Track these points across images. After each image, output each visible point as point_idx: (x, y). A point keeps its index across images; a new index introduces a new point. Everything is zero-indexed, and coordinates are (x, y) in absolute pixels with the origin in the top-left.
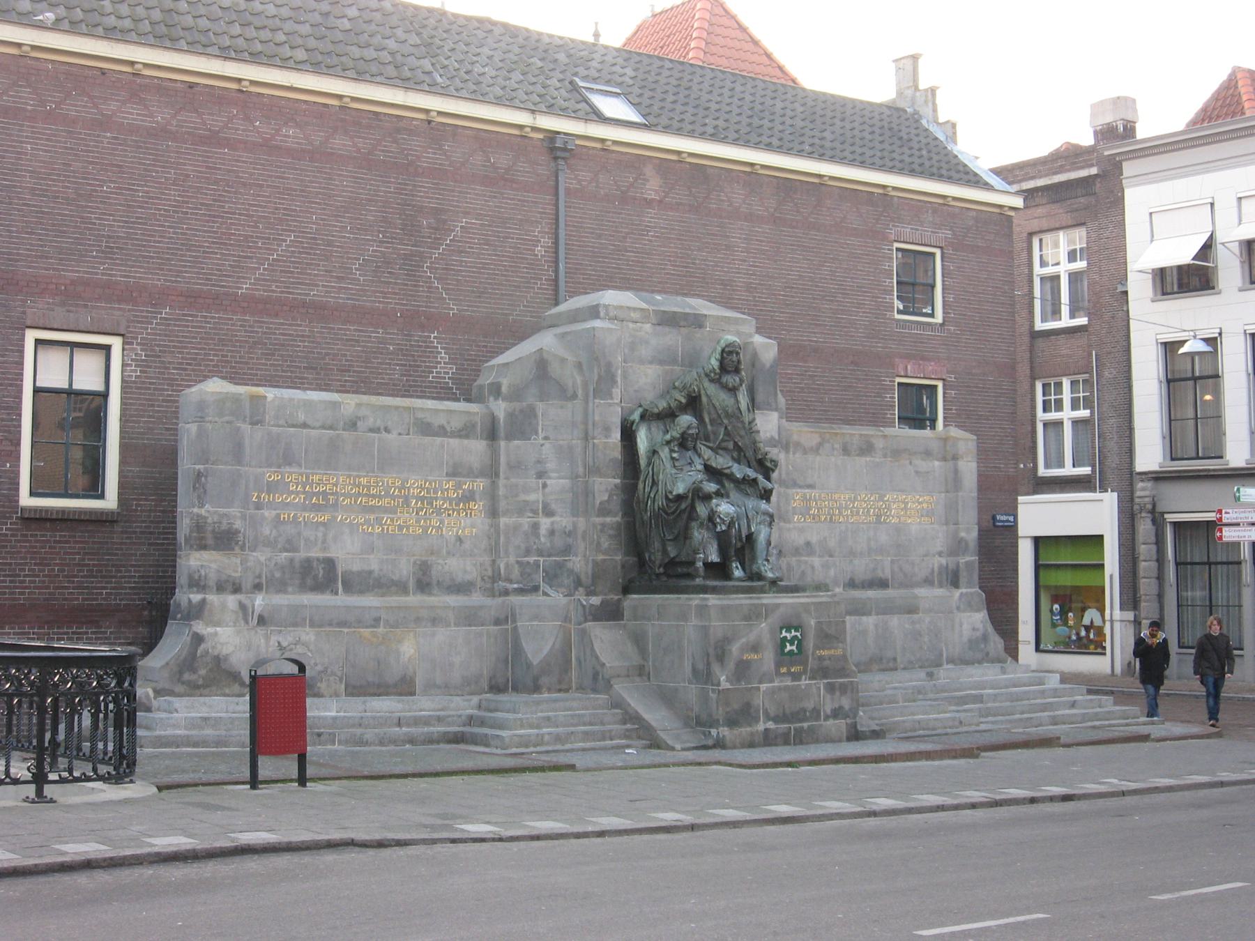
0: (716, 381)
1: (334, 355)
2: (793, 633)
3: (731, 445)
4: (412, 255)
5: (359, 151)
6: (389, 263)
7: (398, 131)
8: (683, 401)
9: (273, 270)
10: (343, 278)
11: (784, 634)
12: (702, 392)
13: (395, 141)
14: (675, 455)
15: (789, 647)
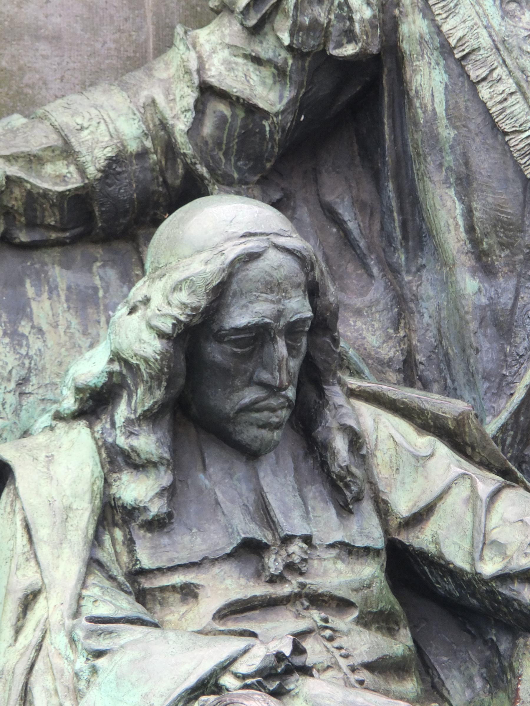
8: (270, 96)
14: (136, 490)
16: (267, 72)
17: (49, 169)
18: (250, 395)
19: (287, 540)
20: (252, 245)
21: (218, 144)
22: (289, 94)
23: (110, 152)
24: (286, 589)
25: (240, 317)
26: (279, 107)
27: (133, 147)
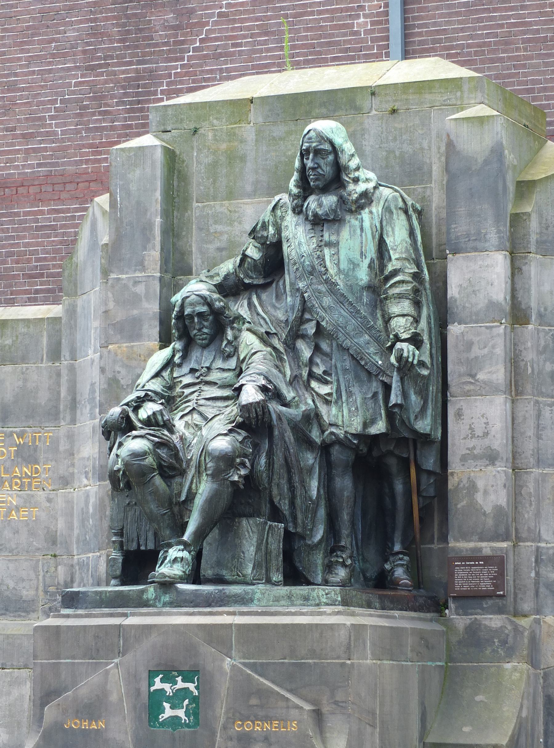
1: (19, 254)
2: (180, 684)
3: (310, 329)
4: (137, 79)
6: (103, 97)
10: (32, 135)
11: (158, 684)
15: (168, 712)
16: (257, 249)
17: (215, 279)
19: (202, 368)
20: (188, 294)
21: (248, 269)
22: (261, 255)
23: (225, 273)
24: (198, 381)
25: (186, 313)
26: (259, 258)
27: (231, 271)
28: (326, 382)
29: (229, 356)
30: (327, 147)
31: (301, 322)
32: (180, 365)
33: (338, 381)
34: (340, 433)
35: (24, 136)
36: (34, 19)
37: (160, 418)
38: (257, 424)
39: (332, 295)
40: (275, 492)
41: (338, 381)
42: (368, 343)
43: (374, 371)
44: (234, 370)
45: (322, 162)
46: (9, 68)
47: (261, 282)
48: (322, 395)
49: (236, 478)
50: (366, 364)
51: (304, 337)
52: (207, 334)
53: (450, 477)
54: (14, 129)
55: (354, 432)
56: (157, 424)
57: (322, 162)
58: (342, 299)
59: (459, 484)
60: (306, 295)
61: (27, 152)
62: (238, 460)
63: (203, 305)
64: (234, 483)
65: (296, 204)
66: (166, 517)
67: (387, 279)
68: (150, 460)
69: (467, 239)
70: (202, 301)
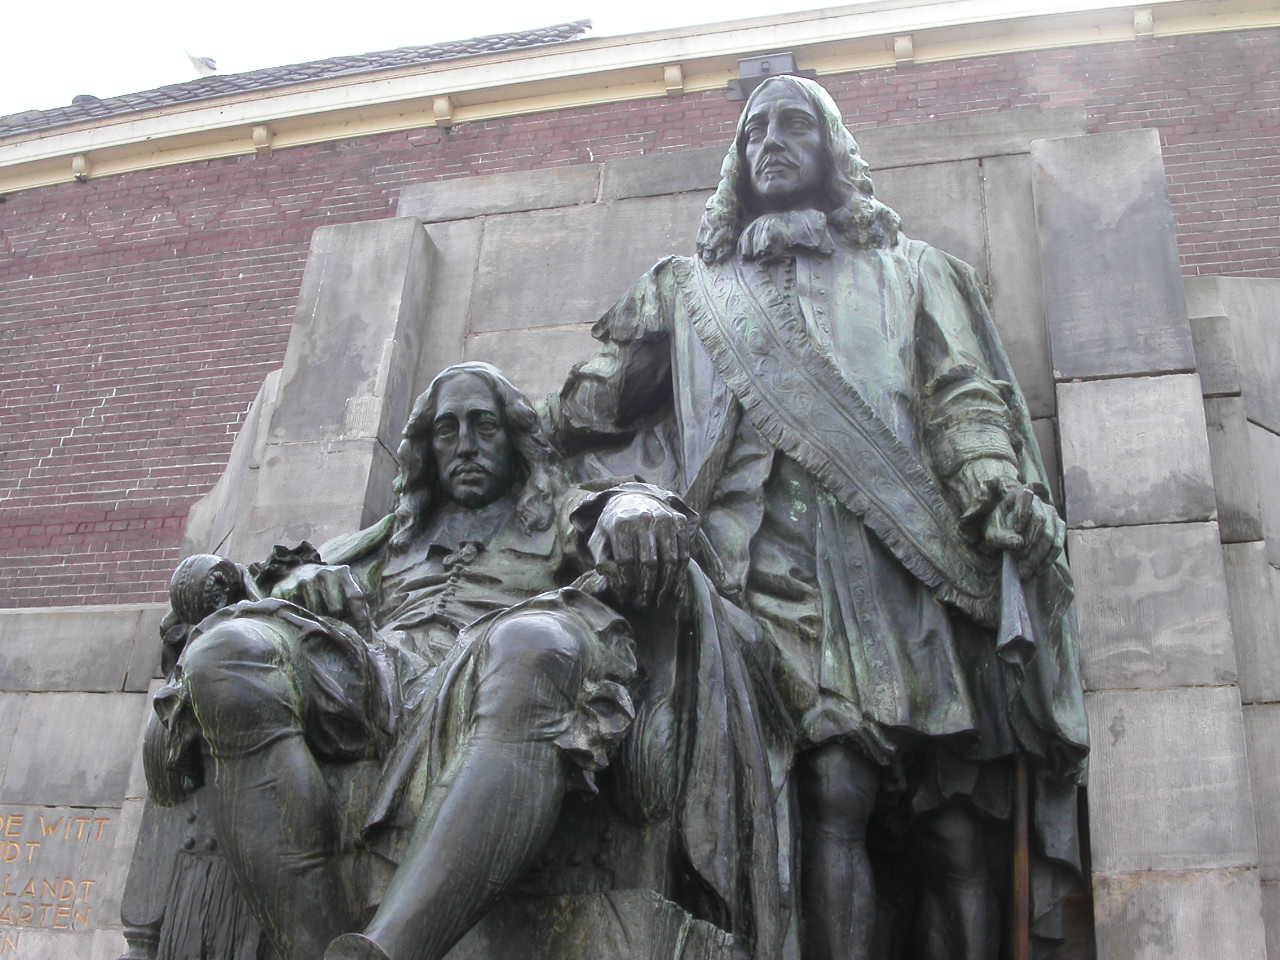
0: (723, 253)
3: (755, 476)
5: (283, 214)
7: (374, 160)
9: (63, 461)
10: (201, 451)
12: (680, 314)
13: (366, 179)
18: (452, 467)
22: (617, 366)
28: (798, 597)
29: (537, 528)
30: (808, 109)
31: (725, 467)
32: (402, 550)
33: (834, 593)
34: (853, 719)
35: (189, 451)
36: (236, 308)
37: (334, 593)
38: (652, 596)
39: (821, 388)
40: (695, 827)
41: (834, 593)
42: (912, 511)
43: (927, 577)
44: (547, 558)
45: (792, 143)
46: (188, 367)
47: (610, 429)
48: (792, 622)
49: (581, 742)
50: (909, 558)
51: (731, 500)
52: (483, 470)
53: (1099, 894)
54: (179, 442)
55: (887, 721)
56: (323, 608)
57: (792, 143)
58: (847, 401)
59: (1125, 910)
60: (746, 402)
61: (190, 472)
62: (591, 688)
63: (485, 397)
64: (571, 761)
65: (721, 237)
66: (307, 882)
67: (945, 384)
68: (278, 681)
69: (1103, 349)
70: (486, 388)
